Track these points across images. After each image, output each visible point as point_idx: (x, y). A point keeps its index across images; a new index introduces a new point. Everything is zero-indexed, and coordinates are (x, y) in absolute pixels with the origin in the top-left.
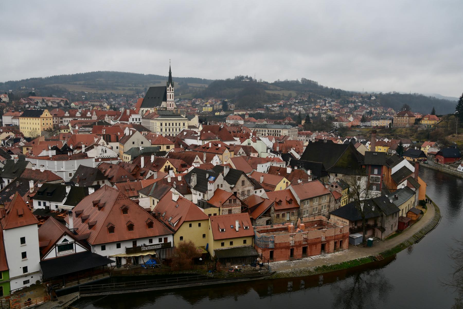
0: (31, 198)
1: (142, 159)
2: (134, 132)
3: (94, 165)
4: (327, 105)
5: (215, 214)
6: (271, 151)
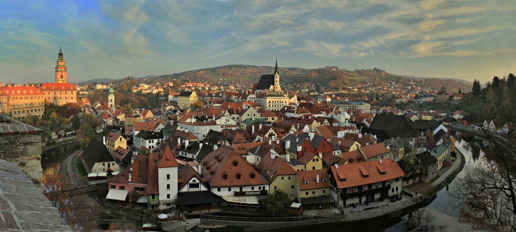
0: (178, 150)
1: (253, 127)
2: (249, 107)
3: (219, 130)
5: (302, 170)
6: (349, 122)
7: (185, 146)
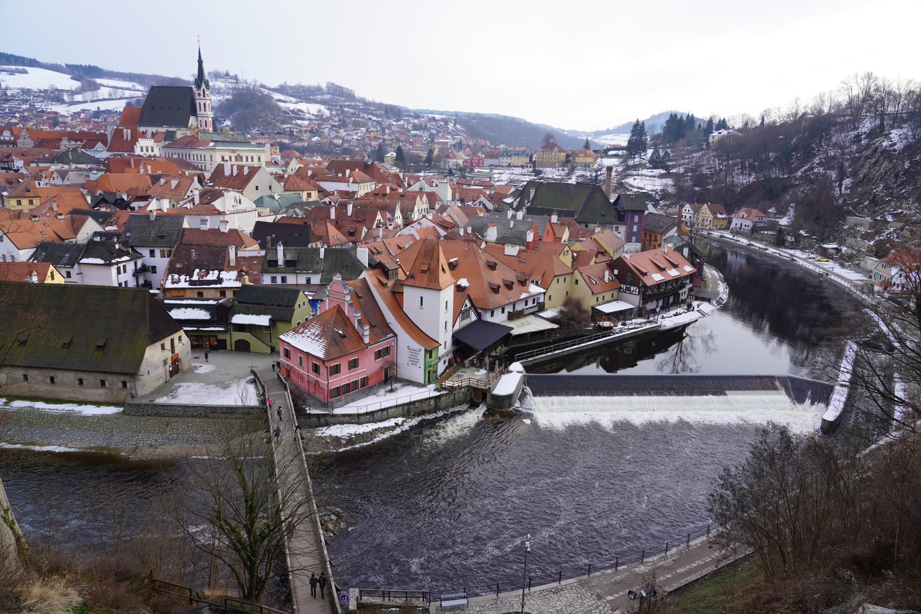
1: (333, 211)
4: (387, 131)
7: (277, 261)
